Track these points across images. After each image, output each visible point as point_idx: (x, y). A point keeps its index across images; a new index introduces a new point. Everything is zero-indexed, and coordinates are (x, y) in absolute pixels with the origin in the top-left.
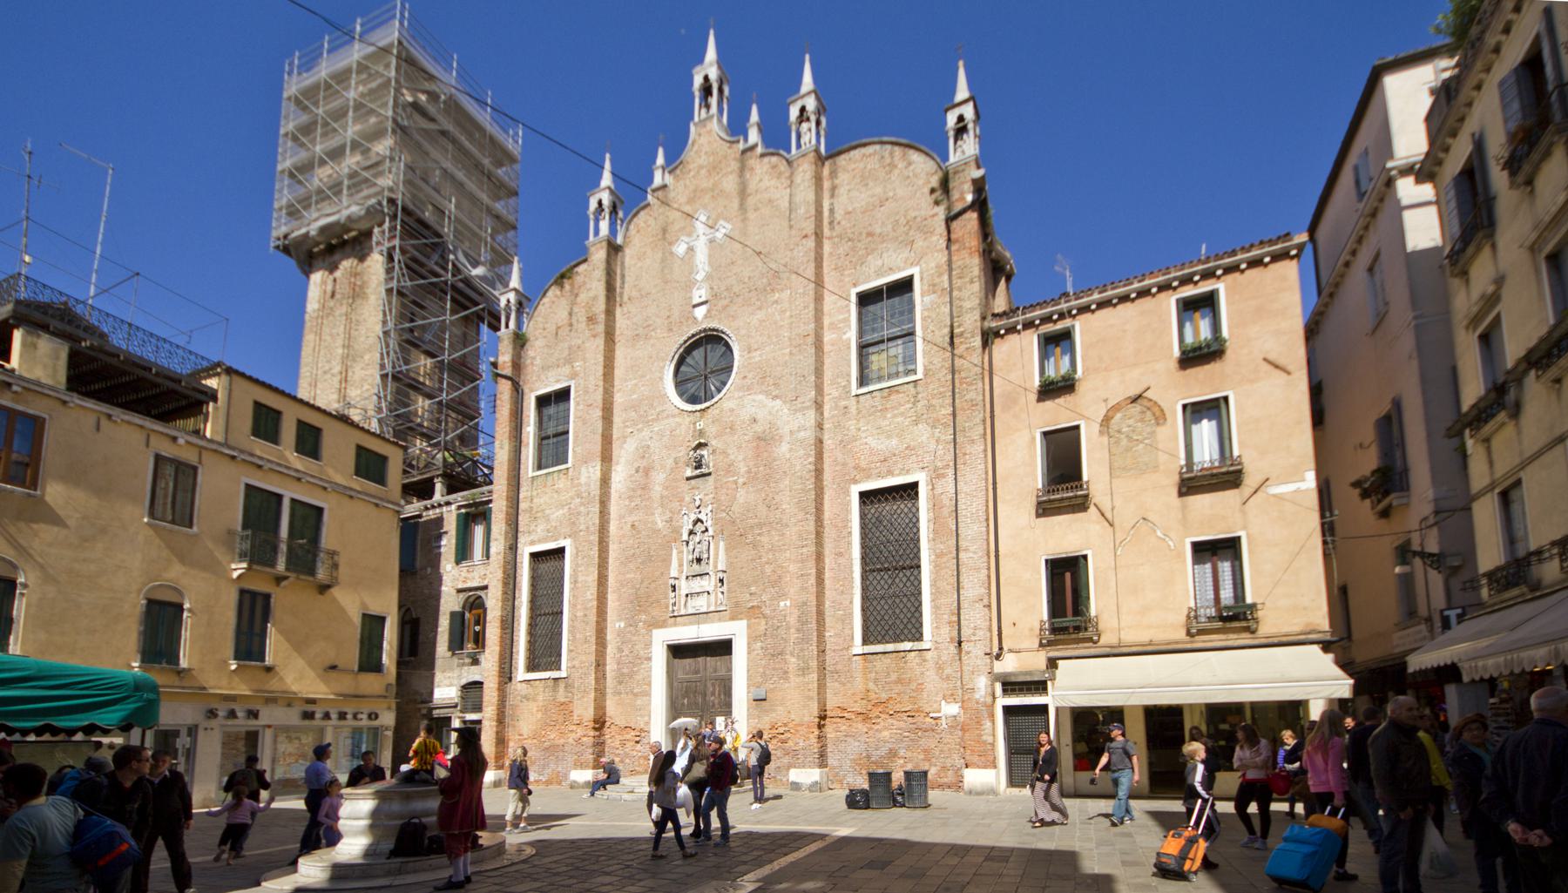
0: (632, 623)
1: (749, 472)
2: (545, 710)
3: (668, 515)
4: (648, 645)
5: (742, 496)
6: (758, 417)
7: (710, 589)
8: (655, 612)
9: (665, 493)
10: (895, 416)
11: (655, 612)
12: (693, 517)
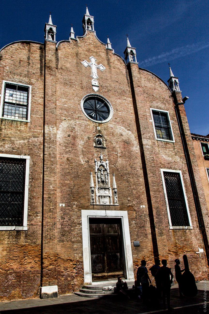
0: (69, 205)
1: (122, 152)
2: (10, 251)
4: (80, 217)
5: (120, 160)
9: (84, 149)
10: (169, 151)
12: (99, 164)
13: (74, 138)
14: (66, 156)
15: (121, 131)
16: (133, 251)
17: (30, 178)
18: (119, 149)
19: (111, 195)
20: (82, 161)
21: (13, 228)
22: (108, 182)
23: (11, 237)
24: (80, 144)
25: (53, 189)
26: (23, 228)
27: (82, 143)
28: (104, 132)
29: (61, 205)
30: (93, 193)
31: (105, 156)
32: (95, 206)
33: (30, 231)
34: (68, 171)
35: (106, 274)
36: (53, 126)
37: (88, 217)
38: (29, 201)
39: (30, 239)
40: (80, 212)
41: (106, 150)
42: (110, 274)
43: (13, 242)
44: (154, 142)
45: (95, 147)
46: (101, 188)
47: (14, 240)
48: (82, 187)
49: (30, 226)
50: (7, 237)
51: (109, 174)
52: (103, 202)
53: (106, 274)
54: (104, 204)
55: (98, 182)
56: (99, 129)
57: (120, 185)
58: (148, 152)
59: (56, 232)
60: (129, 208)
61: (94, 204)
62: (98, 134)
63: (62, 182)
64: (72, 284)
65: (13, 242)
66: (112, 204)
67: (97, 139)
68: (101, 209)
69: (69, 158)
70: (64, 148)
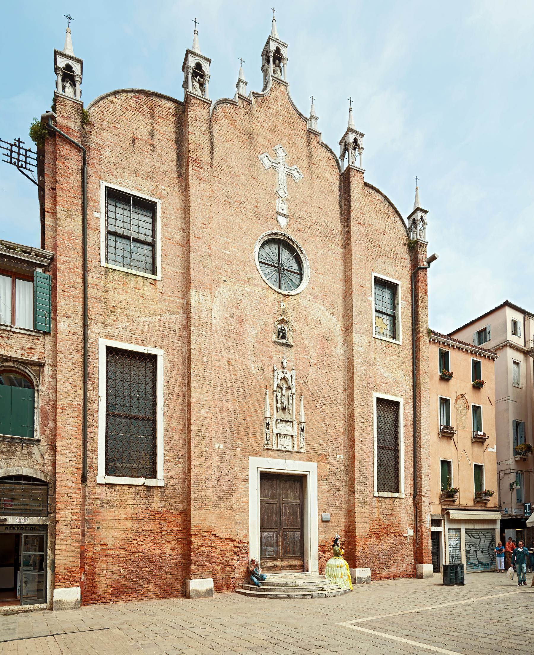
2: (137, 518)
3: (260, 365)
4: (246, 469)
6: (322, 321)
7: (295, 434)
8: (251, 442)
11: (251, 442)
13: (241, 321)
14: (228, 355)
15: (319, 315)
16: (320, 529)
17: (166, 392)
18: (313, 350)
19: (295, 434)
20: (253, 368)
21: (140, 481)
22: (292, 410)
23: (138, 496)
24: (250, 333)
25: (206, 415)
26: (157, 483)
27: (254, 332)
28: (291, 316)
29: (217, 446)
30: (268, 429)
31: (290, 361)
32: (270, 452)
33: (169, 489)
34: (229, 384)
35: (279, 563)
36: (205, 294)
37: (259, 469)
38: (165, 436)
39: (168, 502)
40: (247, 459)
41: (293, 350)
42: (285, 563)
43: (142, 506)
44: (370, 342)
45: (275, 343)
46: (281, 421)
47: (143, 501)
48: (251, 416)
49: (169, 479)
50: (131, 496)
51: (294, 396)
52: (283, 445)
53: (279, 563)
54: (284, 449)
55: (277, 408)
56: (284, 307)
57: (310, 418)
58: (360, 360)
59: (210, 493)
60: (322, 458)
61: (269, 447)
62: (282, 318)
63: (219, 403)
64: (232, 577)
65: (142, 506)
66: (295, 449)
67: (279, 326)
68: (279, 457)
69: (231, 361)
70: (223, 339)
